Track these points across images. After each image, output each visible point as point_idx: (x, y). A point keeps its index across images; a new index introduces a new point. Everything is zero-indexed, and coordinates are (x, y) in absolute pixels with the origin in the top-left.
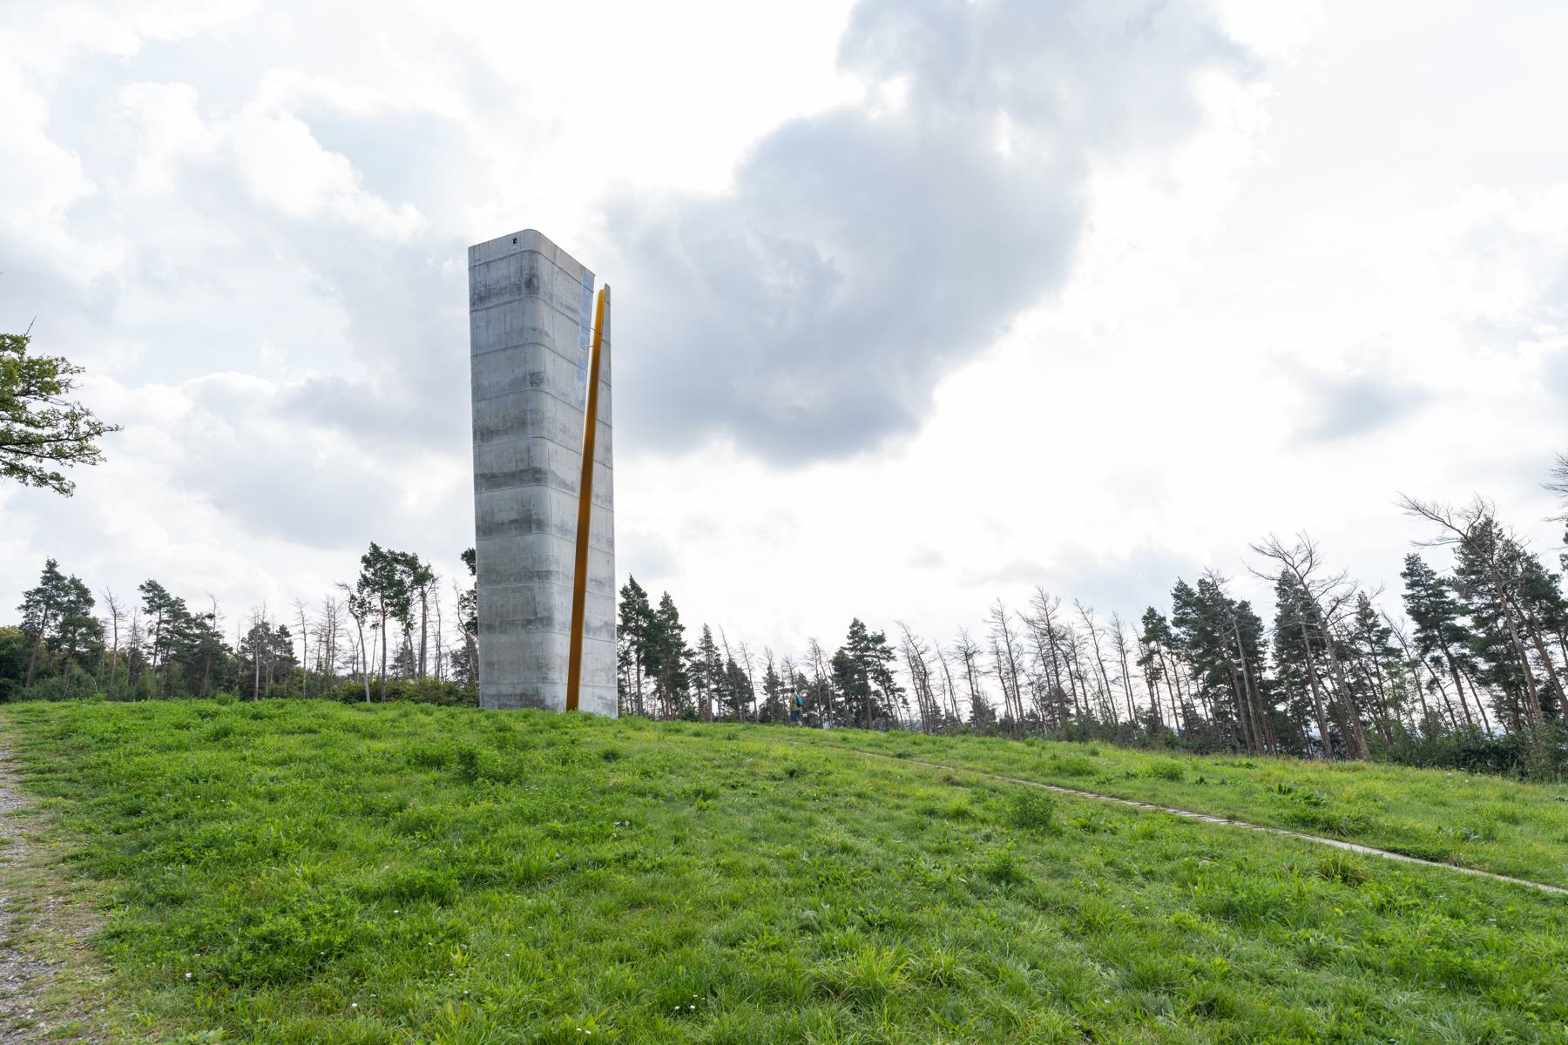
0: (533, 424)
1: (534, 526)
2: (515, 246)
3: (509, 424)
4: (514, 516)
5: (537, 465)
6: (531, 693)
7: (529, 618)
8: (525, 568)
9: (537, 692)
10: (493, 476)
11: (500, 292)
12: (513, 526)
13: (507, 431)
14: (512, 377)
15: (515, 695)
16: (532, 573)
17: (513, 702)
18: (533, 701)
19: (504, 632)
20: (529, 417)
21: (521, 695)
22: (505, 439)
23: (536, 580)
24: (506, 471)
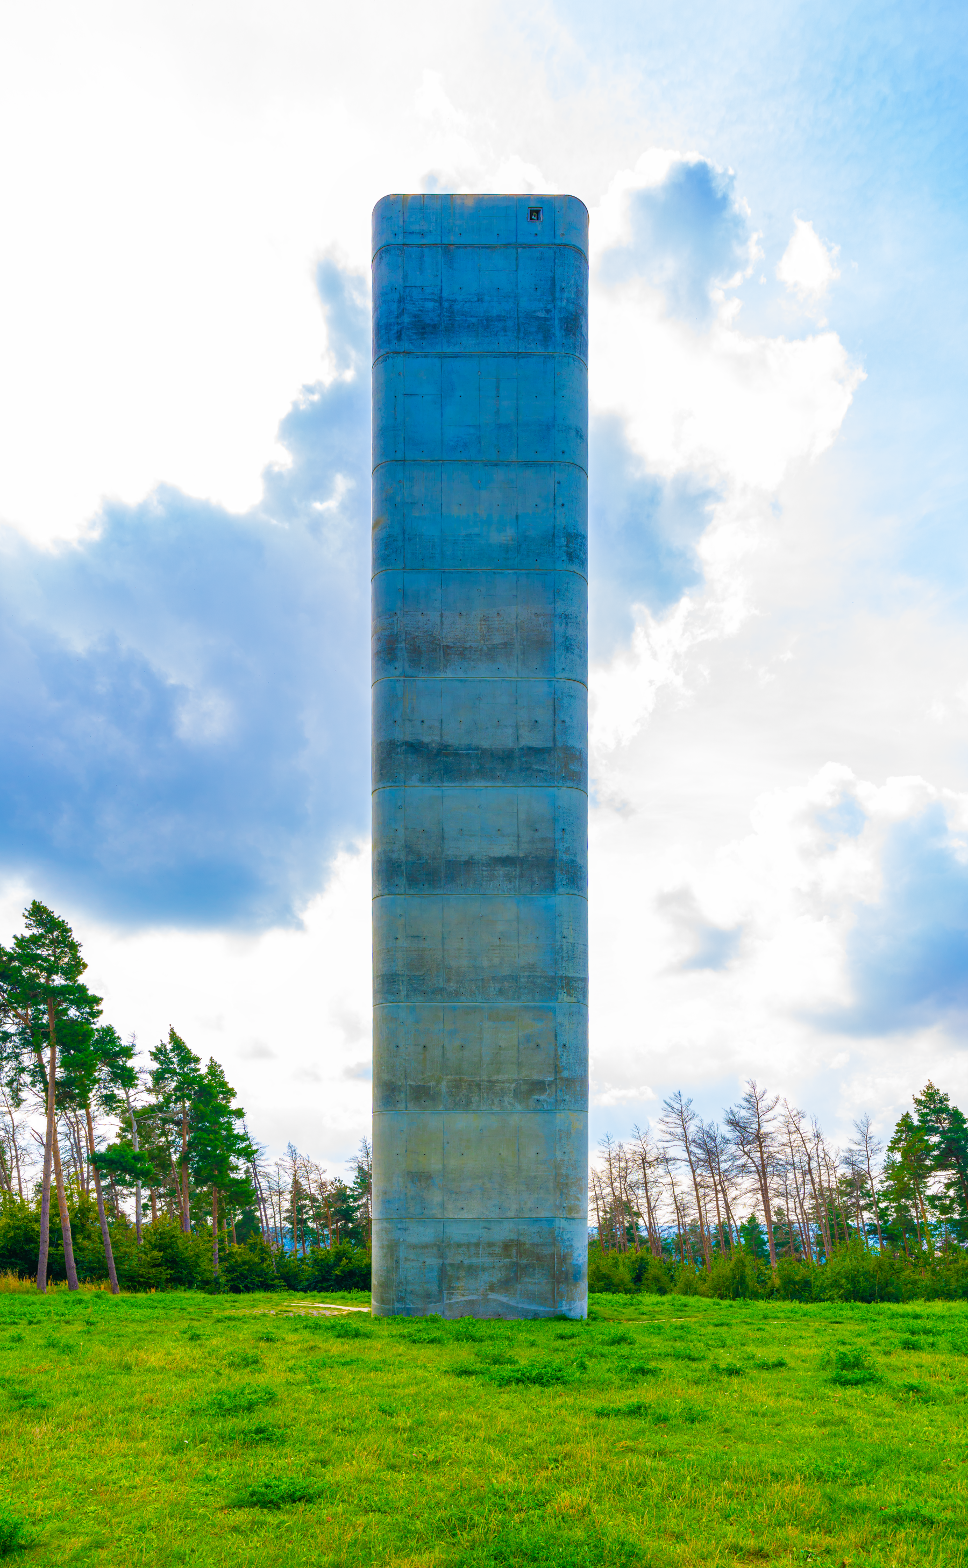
0: (568, 649)
1: (560, 877)
2: (537, 226)
3: (497, 639)
4: (504, 849)
5: (571, 743)
6: (536, 1239)
7: (536, 1077)
8: (532, 967)
9: (555, 1239)
10: (443, 750)
11: (486, 325)
12: (501, 871)
13: (491, 654)
14: (510, 532)
15: (490, 1245)
16: (553, 979)
17: (484, 1260)
18: (539, 1258)
19: (466, 1106)
20: (559, 628)
21: (507, 1246)
22: (483, 670)
23: (563, 997)
24: (485, 744)
